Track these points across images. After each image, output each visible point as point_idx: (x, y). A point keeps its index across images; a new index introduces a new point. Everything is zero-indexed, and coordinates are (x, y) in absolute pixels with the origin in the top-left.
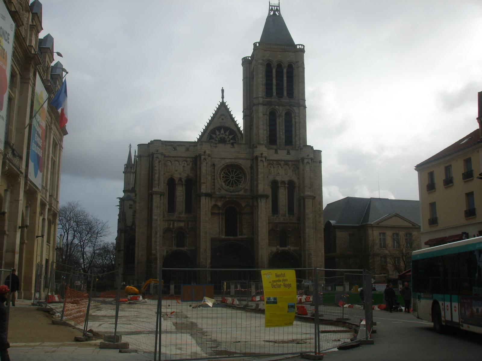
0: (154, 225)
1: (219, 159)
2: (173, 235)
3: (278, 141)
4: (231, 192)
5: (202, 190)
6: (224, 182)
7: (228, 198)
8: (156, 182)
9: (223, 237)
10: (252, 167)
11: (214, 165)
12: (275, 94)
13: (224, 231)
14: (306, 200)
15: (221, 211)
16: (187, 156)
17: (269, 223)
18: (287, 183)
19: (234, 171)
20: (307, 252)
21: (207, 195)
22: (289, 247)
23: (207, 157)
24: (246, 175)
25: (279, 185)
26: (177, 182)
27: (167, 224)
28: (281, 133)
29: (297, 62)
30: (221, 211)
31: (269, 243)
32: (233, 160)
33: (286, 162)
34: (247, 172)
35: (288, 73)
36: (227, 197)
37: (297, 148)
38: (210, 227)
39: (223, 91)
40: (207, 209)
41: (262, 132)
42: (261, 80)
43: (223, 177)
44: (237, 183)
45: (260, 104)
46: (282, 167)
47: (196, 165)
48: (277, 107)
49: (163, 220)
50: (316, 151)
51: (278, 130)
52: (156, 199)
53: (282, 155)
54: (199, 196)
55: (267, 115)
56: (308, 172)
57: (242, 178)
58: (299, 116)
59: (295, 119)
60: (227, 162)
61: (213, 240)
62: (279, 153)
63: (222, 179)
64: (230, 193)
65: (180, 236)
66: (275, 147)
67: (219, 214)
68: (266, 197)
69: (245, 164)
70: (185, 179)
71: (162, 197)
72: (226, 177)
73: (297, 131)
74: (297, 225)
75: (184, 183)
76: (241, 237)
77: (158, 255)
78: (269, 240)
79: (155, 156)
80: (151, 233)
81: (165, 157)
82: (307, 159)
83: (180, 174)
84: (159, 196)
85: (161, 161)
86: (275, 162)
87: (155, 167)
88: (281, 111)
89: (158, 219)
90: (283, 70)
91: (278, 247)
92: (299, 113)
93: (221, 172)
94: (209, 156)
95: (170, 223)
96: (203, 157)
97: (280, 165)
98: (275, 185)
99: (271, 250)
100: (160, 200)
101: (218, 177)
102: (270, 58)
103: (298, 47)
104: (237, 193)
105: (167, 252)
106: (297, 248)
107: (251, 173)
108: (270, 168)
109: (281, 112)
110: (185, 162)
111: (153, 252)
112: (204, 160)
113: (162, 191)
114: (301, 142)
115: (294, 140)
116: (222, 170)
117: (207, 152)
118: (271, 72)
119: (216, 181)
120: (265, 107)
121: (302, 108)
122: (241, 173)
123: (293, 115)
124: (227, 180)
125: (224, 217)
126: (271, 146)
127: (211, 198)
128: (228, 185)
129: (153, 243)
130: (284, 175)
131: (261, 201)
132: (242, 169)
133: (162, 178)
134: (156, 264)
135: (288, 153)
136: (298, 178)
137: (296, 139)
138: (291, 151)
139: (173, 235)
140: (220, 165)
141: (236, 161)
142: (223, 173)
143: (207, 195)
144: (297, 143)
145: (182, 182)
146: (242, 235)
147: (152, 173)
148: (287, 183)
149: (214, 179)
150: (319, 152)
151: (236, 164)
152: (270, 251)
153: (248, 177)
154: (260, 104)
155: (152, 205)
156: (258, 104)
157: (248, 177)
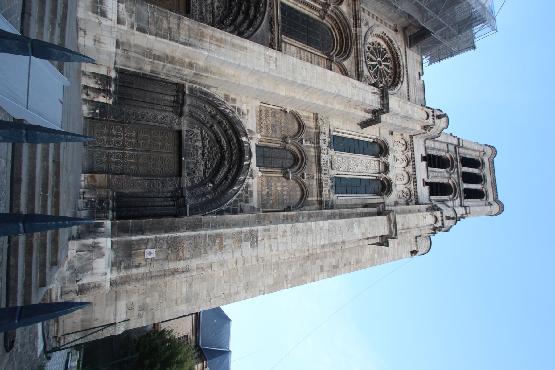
6: (373, 44)
7: (356, 34)
14: (383, 219)
19: (389, 71)
20: (260, 228)
22: (260, 174)
25: (383, 159)
33: (412, 178)
35: (476, 190)
43: (379, 44)
44: (373, 69)
46: (404, 168)
50: (429, 242)
74: (315, 198)
82: (442, 216)
86: (409, 154)
91: (259, 136)
93: (386, 42)
98: (380, 149)
99: (248, 111)
106: (255, 201)
120: (453, 150)
123: (451, 196)
125: (315, 15)
131: (375, 93)
136: (396, 203)
142: (384, 46)
152: (244, 108)
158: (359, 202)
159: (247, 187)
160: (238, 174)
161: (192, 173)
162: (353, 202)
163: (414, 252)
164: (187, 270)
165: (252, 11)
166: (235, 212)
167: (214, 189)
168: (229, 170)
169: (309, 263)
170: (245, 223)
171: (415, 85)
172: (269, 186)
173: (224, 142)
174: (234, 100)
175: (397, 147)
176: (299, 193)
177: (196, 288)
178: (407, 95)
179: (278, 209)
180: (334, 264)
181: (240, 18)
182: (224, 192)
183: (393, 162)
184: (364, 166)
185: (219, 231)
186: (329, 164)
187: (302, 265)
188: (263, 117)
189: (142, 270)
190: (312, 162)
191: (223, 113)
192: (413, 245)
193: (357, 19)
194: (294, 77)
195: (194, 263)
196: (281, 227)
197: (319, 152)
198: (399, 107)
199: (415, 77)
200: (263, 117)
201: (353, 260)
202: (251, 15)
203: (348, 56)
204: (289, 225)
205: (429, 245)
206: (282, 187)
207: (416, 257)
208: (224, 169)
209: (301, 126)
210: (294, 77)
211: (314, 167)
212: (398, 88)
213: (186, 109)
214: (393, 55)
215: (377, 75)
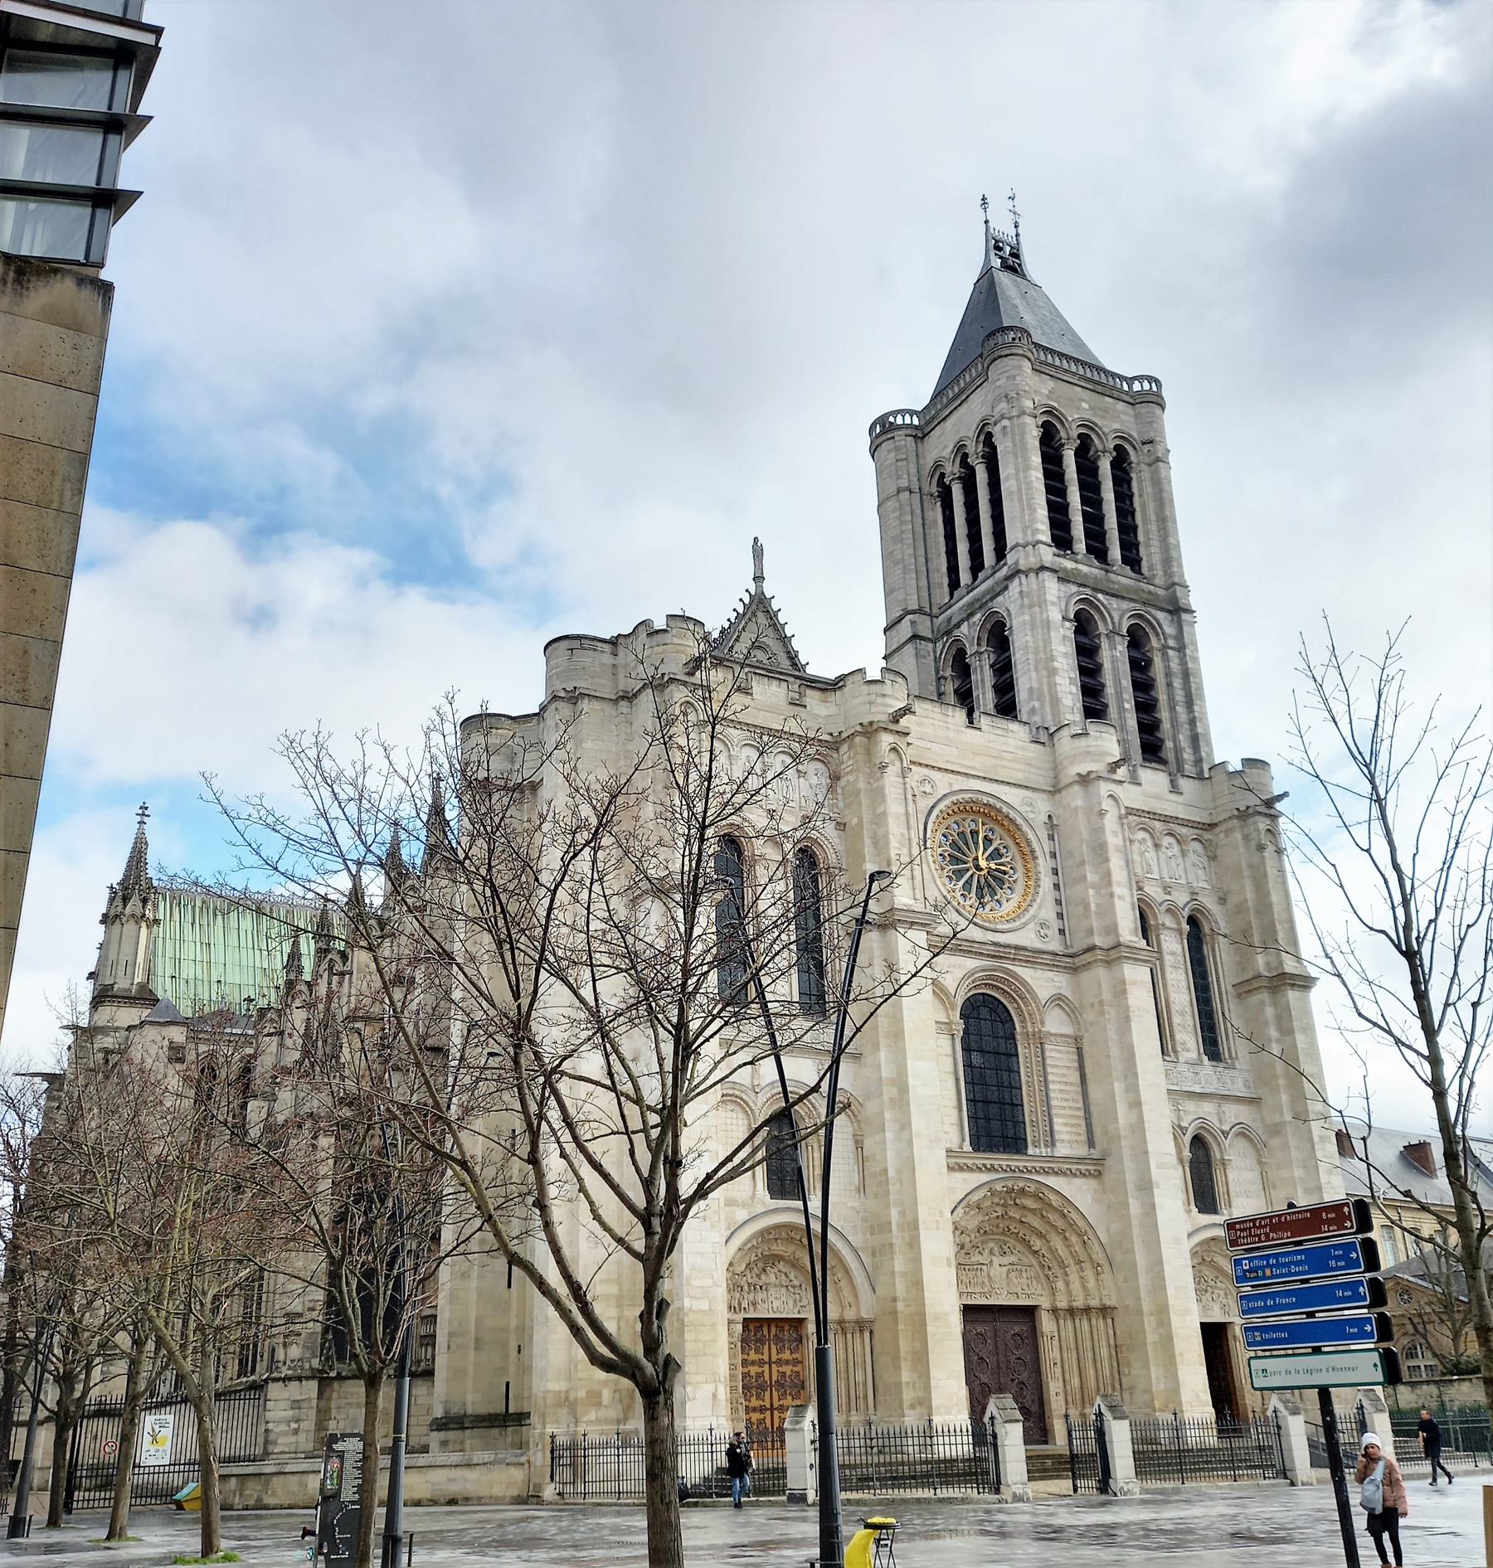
18: (1186, 913)
24: (1035, 858)
34: (1035, 845)
39: (758, 552)
48: (1100, 596)
59: (1165, 656)
88: (1117, 614)
115: (1169, 744)
120: (1062, 587)
123: (1154, 643)
144: (1186, 756)
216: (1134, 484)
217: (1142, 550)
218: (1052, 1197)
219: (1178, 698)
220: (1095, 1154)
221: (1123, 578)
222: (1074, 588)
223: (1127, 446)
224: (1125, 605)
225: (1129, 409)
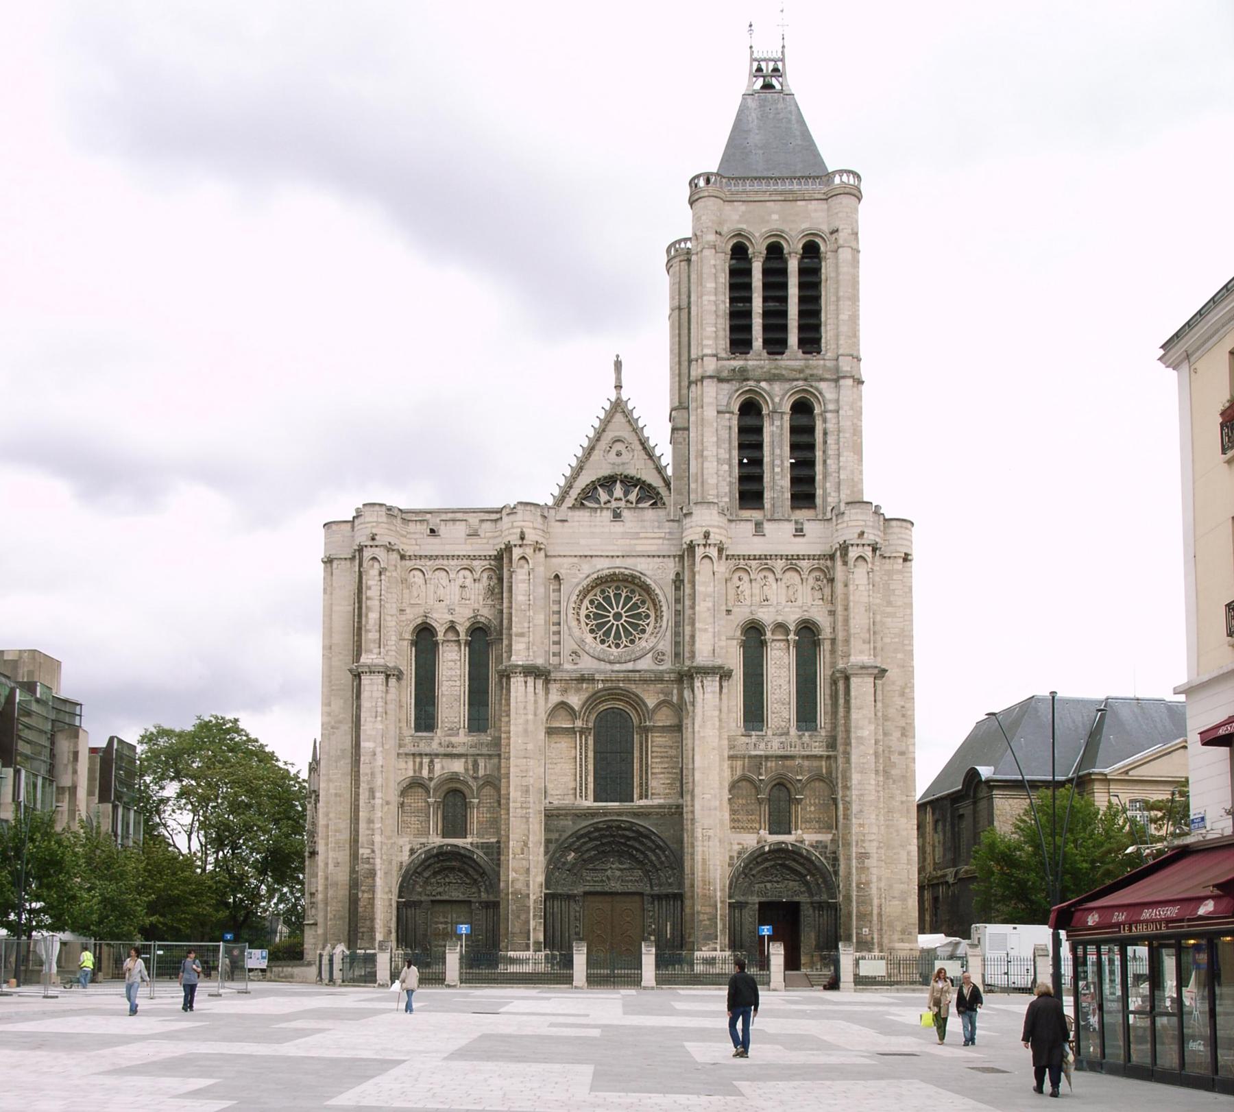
0: (364, 769)
1: (575, 560)
2: (431, 800)
3: (767, 495)
4: (610, 663)
5: (513, 658)
6: (592, 631)
8: (373, 635)
9: (589, 803)
10: (678, 582)
11: (557, 577)
12: (758, 342)
13: (591, 786)
15: (579, 723)
16: (471, 554)
17: (731, 757)
18: (792, 628)
20: (854, 849)
21: (532, 672)
22: (799, 832)
23: (529, 551)
25: (769, 635)
26: (440, 637)
27: (411, 764)
28: (777, 470)
29: (832, 233)
30: (579, 723)
31: (733, 820)
32: (618, 562)
33: (792, 562)
34: (661, 598)
35: (802, 271)
36: (597, 677)
37: (829, 516)
38: (544, 772)
40: (531, 717)
41: (717, 467)
42: (713, 298)
43: (588, 617)
44: (631, 634)
45: (710, 377)
47: (501, 580)
48: (763, 384)
49: (398, 754)
50: (894, 523)
51: (766, 460)
52: (372, 686)
53: (779, 537)
54: (505, 675)
55: (732, 413)
56: (861, 588)
57: (648, 616)
58: (838, 412)
59: (825, 421)
60: (599, 567)
61: (551, 815)
62: (766, 532)
63: (583, 624)
64: (609, 667)
65: (454, 802)
66: (756, 515)
67: (572, 731)
68: (724, 675)
69: (658, 574)
70: (468, 624)
71: (393, 681)
72: (597, 616)
73: (829, 462)
75: (463, 636)
76: (643, 802)
77: (378, 861)
78: (733, 811)
79: (367, 554)
80: (357, 794)
81: (403, 557)
83: (451, 611)
84: (382, 676)
85: (385, 569)
86: (754, 563)
87: (369, 588)
88: (778, 398)
89: (379, 750)
90: (786, 262)
92: (837, 401)
93: (582, 601)
94: (540, 549)
95: (421, 763)
96: (517, 553)
97: (771, 570)
98: (754, 637)
100: (387, 692)
101: (570, 616)
102: (744, 226)
103: (837, 180)
104: (630, 666)
105: (412, 851)
106: (826, 837)
107: (677, 601)
108: (739, 583)
109: (777, 400)
110: (467, 573)
111: (364, 852)
112: (523, 561)
113: (391, 665)
114: (843, 496)
115: (819, 492)
116: (585, 593)
117: (531, 537)
118: (748, 272)
119: (564, 628)
120: (725, 386)
121: (849, 382)
122: (643, 602)
124: (600, 626)
126: (746, 514)
127: (547, 682)
128: (603, 642)
129: (362, 826)
130: (786, 601)
132: (646, 589)
133: (391, 623)
134: (372, 889)
135: (799, 532)
136: (832, 613)
137: (828, 485)
138: (807, 527)
139: (431, 800)
140: (579, 575)
141: (629, 562)
143: (532, 672)
144: (829, 499)
145: (458, 635)
146: (647, 797)
147: (360, 608)
148: (792, 628)
149: (559, 624)
150: (904, 524)
151: (627, 572)
152: (737, 847)
153: (667, 614)
154: (710, 377)
155: (359, 707)
156: (703, 378)
157: (664, 614)
158: (828, 691)
159: (812, 846)
160: (801, 855)
161: (796, 893)
162: (828, 702)
163: (906, 558)
164: (880, 906)
165: (627, 833)
166: (836, 859)
167: (813, 875)
168: (794, 860)
169: (893, 772)
170: (849, 859)
171: (636, 536)
172: (810, 821)
173: (767, 864)
174: (731, 858)
175: (747, 593)
176: (817, 784)
177: (896, 894)
178: (656, 559)
179: (833, 808)
180: (897, 734)
181: (637, 845)
182: (816, 868)
183: (771, 609)
184: (780, 667)
185: (854, 885)
186: (783, 739)
187: (894, 782)
188: (741, 825)
189: (875, 936)
190: (783, 766)
191: (744, 868)
192: (896, 567)
193: (582, 679)
194: (715, 809)
195: (876, 902)
196: (855, 830)
197: (772, 757)
198: (706, 630)
199: (625, 535)
200: (741, 825)
201: (899, 702)
202: (632, 835)
203: (637, 696)
204: (854, 820)
205: (899, 523)
206: (811, 805)
207: (915, 555)
208: (793, 864)
209: (744, 778)
210: (715, 809)
211: (788, 763)
212: (653, 586)
213: (742, 899)
214: (597, 585)
215: (639, 625)
216: (823, 270)
217: (823, 328)
218: (641, 830)
219: (830, 452)
220: (680, 801)
221: (793, 356)
222: (735, 385)
223: (818, 240)
224: (787, 386)
225: (823, 205)
